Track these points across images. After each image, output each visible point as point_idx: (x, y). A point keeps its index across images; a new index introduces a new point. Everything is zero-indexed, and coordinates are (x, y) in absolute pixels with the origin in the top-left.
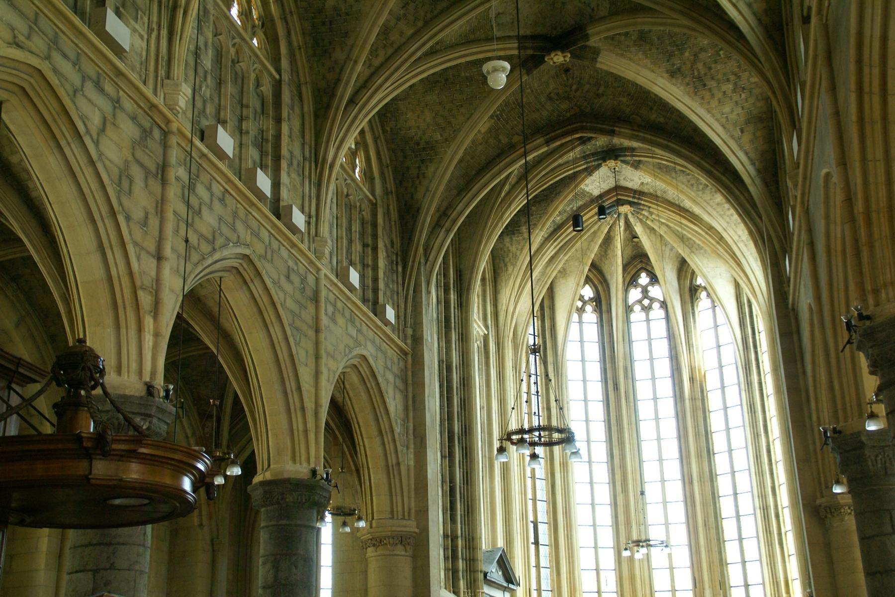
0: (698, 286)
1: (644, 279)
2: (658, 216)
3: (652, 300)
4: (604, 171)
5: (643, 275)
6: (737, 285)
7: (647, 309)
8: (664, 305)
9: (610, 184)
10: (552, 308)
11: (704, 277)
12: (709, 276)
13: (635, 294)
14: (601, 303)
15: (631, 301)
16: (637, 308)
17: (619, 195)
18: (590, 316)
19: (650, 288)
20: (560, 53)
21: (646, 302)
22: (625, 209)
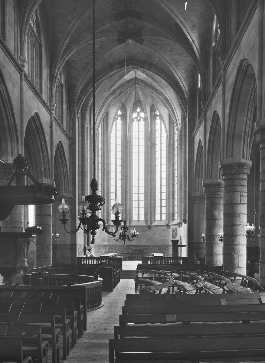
0: (157, 114)
1: (139, 110)
2: (148, 89)
3: (141, 118)
4: (132, 72)
5: (139, 108)
6: (170, 116)
7: (139, 121)
8: (145, 120)
9: (133, 76)
11: (160, 112)
12: (161, 112)
13: (135, 115)
14: (124, 117)
16: (135, 120)
17: (136, 80)
18: (119, 122)
19: (140, 113)
20: (132, 40)
21: (139, 118)
22: (137, 85)
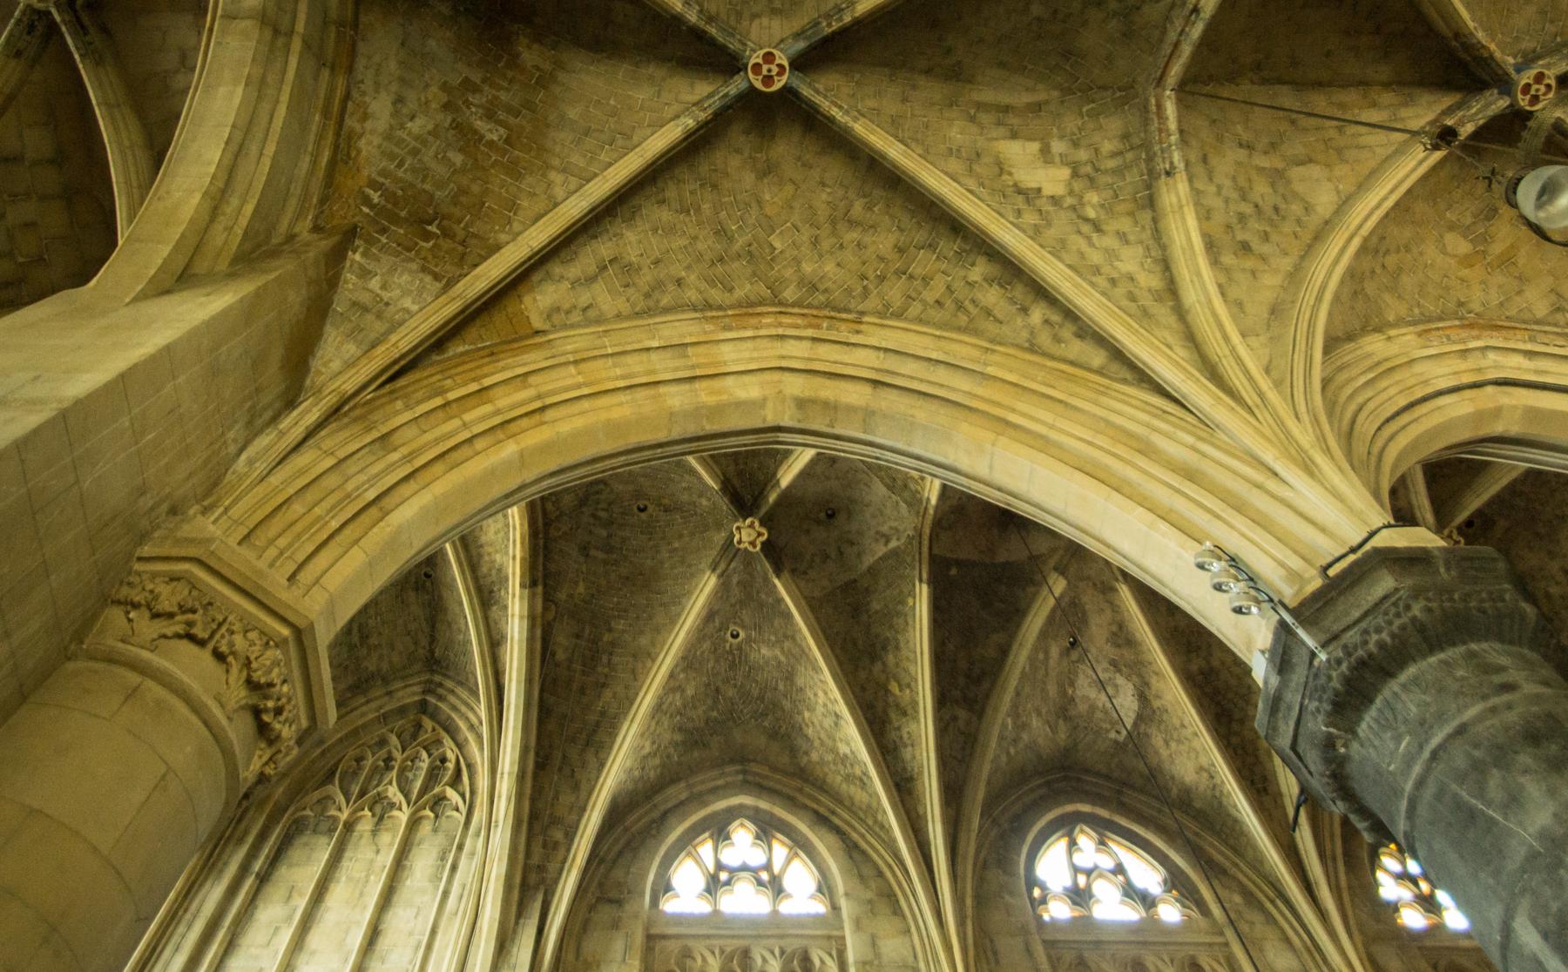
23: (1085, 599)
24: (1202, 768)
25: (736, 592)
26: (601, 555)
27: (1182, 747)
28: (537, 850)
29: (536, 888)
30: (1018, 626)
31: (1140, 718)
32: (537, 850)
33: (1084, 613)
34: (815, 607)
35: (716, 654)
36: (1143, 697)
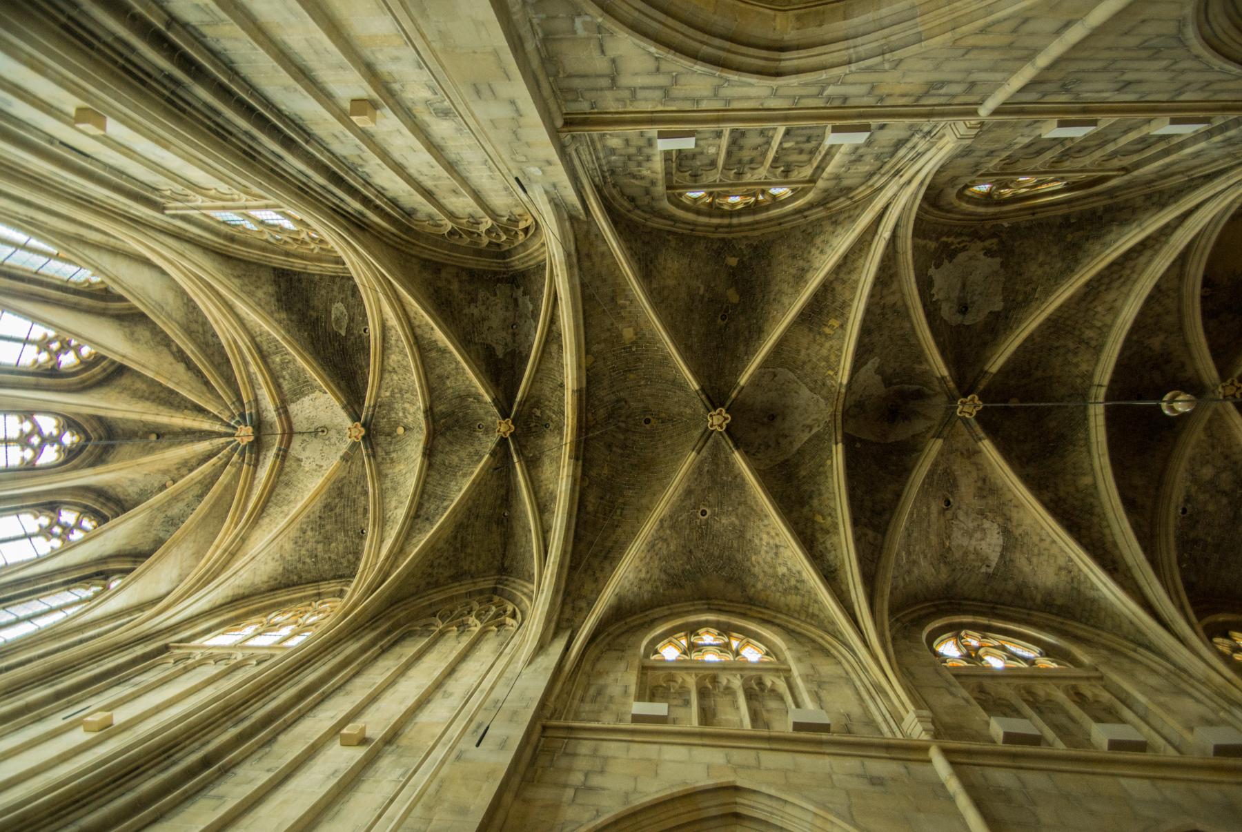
1: (69, 439)
3: (39, 450)
5: (76, 439)
7: (24, 441)
10: (101, 313)
13: (49, 425)
15: (38, 418)
16: (27, 427)
19: (56, 446)
23: (955, 467)
24: (1060, 569)
25: (706, 479)
26: (620, 451)
27: (1042, 558)
28: (568, 610)
29: (567, 628)
30: (908, 478)
31: (1005, 549)
32: (568, 610)
33: (955, 479)
34: (763, 476)
35: (690, 522)
36: (1006, 532)
